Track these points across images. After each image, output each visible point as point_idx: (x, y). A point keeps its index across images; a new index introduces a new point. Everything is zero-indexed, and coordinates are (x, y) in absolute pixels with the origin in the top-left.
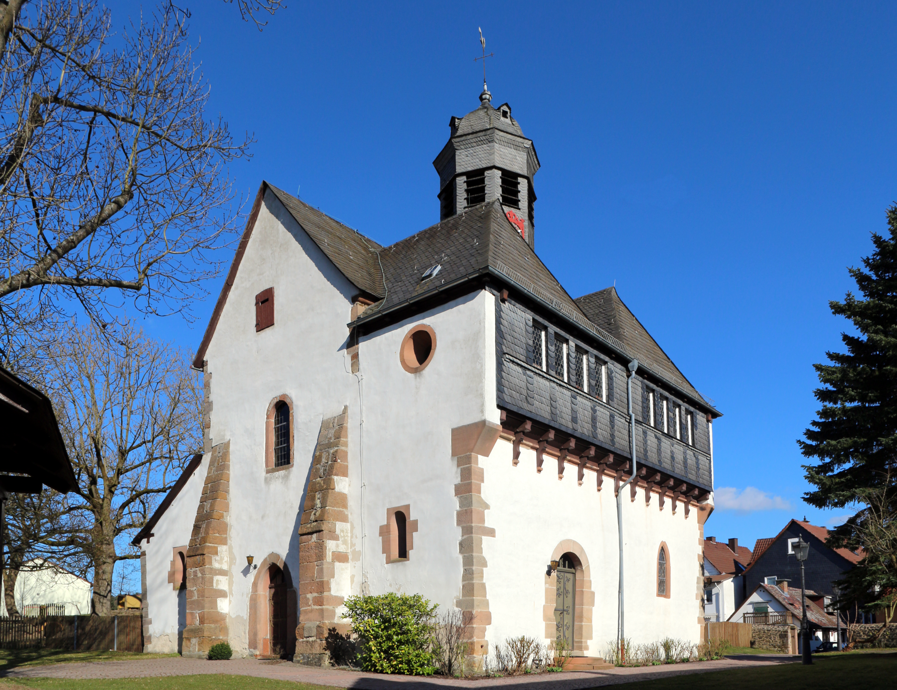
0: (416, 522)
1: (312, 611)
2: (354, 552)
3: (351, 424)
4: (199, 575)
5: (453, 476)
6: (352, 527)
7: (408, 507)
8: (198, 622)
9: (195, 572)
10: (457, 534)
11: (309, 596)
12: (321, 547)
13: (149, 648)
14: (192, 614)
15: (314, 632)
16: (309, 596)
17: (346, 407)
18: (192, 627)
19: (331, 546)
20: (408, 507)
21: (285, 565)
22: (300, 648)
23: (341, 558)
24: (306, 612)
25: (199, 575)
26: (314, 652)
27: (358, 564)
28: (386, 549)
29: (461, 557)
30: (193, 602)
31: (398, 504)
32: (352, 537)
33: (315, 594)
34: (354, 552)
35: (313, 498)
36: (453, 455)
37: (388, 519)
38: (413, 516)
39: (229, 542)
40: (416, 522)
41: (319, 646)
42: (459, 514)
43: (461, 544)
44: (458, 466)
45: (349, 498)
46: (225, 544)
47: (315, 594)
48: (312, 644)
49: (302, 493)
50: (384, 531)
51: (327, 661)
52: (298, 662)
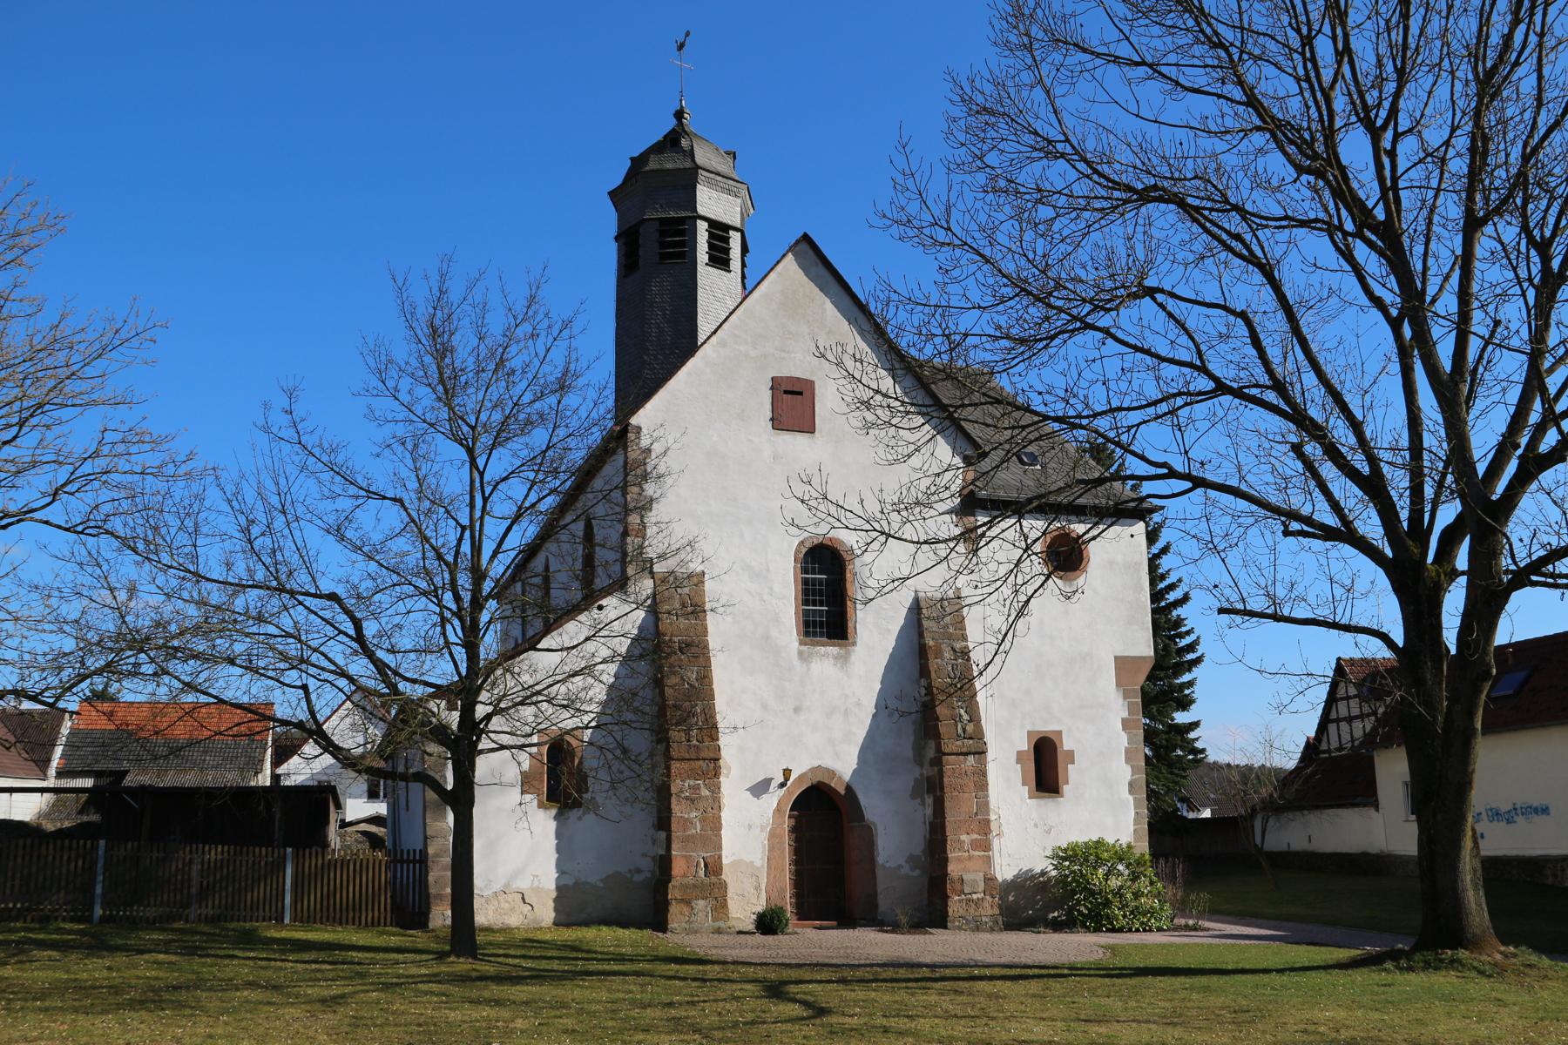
7: (1060, 733)
11: (964, 837)
14: (688, 858)
16: (964, 837)
18: (690, 880)
20: (1060, 733)
21: (849, 788)
22: (955, 906)
24: (959, 860)
25: (705, 792)
30: (687, 840)
33: (975, 836)
36: (1118, 685)
38: (1067, 744)
42: (1127, 751)
43: (1130, 784)
44: (1125, 698)
47: (975, 836)
48: (977, 903)
52: (960, 928)
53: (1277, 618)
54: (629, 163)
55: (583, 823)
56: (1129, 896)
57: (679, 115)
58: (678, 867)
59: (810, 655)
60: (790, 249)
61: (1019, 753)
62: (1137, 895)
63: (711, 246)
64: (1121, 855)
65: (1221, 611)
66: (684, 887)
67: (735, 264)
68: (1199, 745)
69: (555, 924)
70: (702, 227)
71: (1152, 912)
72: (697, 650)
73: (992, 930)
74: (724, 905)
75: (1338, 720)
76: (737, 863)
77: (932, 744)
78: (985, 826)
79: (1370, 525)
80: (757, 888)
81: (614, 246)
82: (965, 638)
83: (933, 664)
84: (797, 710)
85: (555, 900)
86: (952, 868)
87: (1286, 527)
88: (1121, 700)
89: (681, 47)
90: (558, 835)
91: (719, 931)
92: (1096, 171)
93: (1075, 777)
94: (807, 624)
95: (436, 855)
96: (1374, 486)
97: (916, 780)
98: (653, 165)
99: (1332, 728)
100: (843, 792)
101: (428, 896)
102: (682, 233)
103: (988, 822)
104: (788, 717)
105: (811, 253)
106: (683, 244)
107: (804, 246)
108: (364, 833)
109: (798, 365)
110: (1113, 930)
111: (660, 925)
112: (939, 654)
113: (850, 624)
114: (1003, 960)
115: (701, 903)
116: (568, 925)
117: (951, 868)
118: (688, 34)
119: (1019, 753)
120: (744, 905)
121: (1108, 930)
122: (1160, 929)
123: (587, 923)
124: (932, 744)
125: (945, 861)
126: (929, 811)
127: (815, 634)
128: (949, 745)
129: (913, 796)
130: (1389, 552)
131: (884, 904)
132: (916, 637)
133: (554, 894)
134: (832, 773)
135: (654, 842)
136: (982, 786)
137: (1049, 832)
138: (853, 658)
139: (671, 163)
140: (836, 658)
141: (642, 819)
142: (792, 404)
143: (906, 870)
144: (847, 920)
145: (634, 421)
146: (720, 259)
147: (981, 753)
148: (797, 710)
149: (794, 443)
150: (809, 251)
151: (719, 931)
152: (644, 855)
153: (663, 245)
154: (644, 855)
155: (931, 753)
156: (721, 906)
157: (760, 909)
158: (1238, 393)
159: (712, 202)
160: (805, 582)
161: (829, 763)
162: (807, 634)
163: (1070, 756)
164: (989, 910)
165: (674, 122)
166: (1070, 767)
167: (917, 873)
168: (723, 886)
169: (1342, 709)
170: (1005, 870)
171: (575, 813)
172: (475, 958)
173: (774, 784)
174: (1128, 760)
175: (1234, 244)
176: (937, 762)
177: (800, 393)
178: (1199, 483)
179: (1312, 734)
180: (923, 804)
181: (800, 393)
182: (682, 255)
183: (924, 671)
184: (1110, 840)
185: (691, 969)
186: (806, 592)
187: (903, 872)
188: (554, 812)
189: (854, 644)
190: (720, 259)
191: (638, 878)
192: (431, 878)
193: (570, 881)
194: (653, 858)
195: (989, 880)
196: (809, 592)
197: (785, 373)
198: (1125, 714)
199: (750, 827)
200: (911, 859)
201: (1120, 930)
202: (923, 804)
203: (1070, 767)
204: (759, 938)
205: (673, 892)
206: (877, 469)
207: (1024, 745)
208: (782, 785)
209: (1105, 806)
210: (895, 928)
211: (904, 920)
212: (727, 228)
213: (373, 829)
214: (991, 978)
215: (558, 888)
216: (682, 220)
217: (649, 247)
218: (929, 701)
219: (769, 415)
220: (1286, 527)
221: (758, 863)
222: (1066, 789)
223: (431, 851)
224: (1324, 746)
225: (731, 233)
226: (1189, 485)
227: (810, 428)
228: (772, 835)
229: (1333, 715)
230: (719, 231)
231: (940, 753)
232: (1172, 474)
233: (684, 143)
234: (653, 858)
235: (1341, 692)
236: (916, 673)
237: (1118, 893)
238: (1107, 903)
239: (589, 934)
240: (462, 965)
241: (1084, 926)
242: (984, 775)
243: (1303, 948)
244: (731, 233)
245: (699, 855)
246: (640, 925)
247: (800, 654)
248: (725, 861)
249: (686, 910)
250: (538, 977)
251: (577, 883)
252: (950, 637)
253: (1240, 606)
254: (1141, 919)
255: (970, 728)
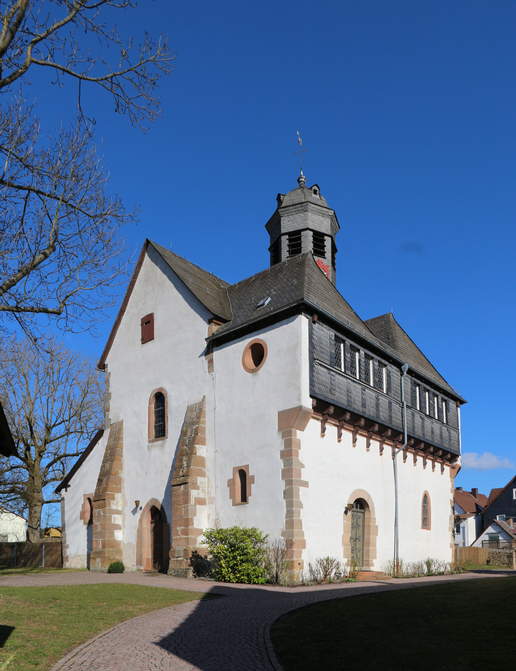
0: (253, 477)
1: (180, 539)
2: (210, 498)
3: (208, 408)
4: (102, 514)
5: (279, 445)
6: (209, 481)
7: (247, 466)
8: (101, 547)
9: (99, 512)
10: (282, 485)
11: (179, 528)
12: (187, 494)
13: (67, 565)
14: (97, 541)
15: (182, 554)
16: (179, 528)
17: (204, 397)
18: (97, 550)
19: (194, 494)
20: (247, 466)
21: (162, 507)
22: (172, 564)
23: (201, 502)
24: (176, 539)
26: (182, 568)
27: (213, 506)
28: (232, 496)
29: (284, 502)
31: (240, 464)
32: (208, 487)
33: (183, 528)
34: (210, 498)
35: (181, 460)
36: (279, 430)
37: (234, 475)
38: (251, 473)
39: (122, 491)
40: (253, 477)
41: (185, 564)
42: (283, 472)
43: (284, 492)
44: (283, 438)
45: (206, 460)
46: (120, 492)
47: (183, 528)
48: (181, 562)
49: (174, 456)
50: (231, 483)
51: (191, 574)
52: (171, 574)
100: (159, 509)
166: (252, 485)
203: (252, 485)
249: (94, 562)
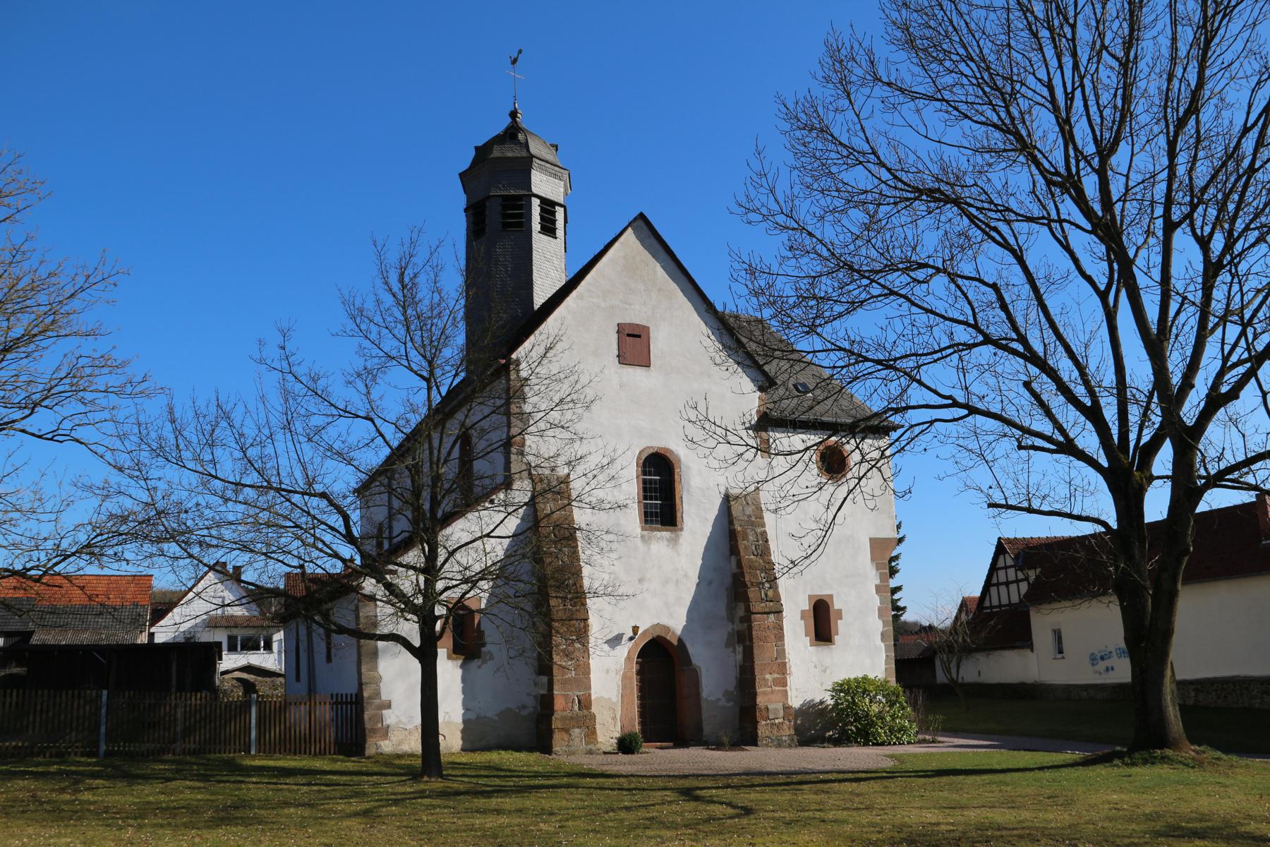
0: (840, 611)
7: (831, 596)
11: (768, 676)
14: (566, 697)
16: (768, 676)
18: (568, 713)
20: (831, 596)
21: (680, 640)
22: (763, 729)
24: (765, 693)
30: (565, 682)
33: (776, 675)
36: (873, 559)
38: (837, 605)
40: (840, 611)
42: (880, 609)
43: (882, 634)
47: (776, 675)
48: (779, 726)
49: (700, 562)
52: (767, 745)
53: (1030, 510)
54: (473, 153)
55: (483, 670)
56: (888, 719)
57: (513, 114)
58: (559, 704)
59: (650, 538)
60: (630, 225)
61: (803, 612)
62: (893, 717)
63: (542, 218)
64: (882, 687)
65: (990, 505)
66: (564, 719)
67: (560, 233)
68: (900, 604)
69: (463, 750)
70: (536, 203)
71: (902, 729)
72: (567, 535)
73: (790, 746)
74: (594, 732)
75: (998, 584)
76: (597, 699)
77: (742, 606)
78: (782, 668)
79: (1089, 440)
80: (614, 718)
81: (463, 215)
82: (763, 525)
83: (742, 545)
84: (641, 581)
85: (463, 731)
86: (761, 701)
87: (1020, 443)
88: (874, 571)
89: (514, 61)
90: (464, 680)
91: (590, 752)
92: (895, 177)
93: (844, 629)
94: (646, 514)
95: (370, 698)
96: (1093, 414)
97: (729, 634)
98: (496, 153)
99: (993, 590)
100: (675, 643)
101: (364, 730)
102: (521, 207)
103: (785, 664)
104: (640, 586)
105: (645, 228)
106: (521, 216)
107: (640, 223)
108: (238, 679)
109: (635, 316)
110: (877, 744)
111: (546, 748)
112: (745, 537)
113: (678, 515)
114: (865, 768)
115: (577, 730)
116: (473, 751)
117: (759, 700)
118: (520, 52)
119: (803, 612)
120: (608, 732)
121: (874, 744)
122: (909, 743)
123: (489, 749)
124: (742, 606)
125: (754, 695)
126: (740, 657)
127: (652, 522)
128: (757, 606)
129: (727, 646)
130: (1106, 464)
131: (707, 729)
132: (726, 524)
133: (461, 726)
134: (667, 629)
135: (536, 684)
136: (780, 637)
137: (825, 671)
138: (681, 541)
139: (511, 152)
140: (668, 540)
141: (524, 670)
142: (633, 344)
143: (723, 702)
144: (680, 740)
145: (514, 356)
146: (549, 228)
147: (779, 612)
148: (641, 581)
149: (635, 373)
150: (644, 226)
151: (590, 752)
152: (529, 695)
153: (505, 216)
154: (529, 695)
155: (741, 612)
156: (591, 733)
157: (618, 735)
158: (996, 343)
159: (543, 184)
160: (645, 482)
161: (665, 621)
162: (646, 522)
163: (839, 614)
164: (787, 732)
165: (509, 120)
167: (731, 704)
168: (593, 717)
169: (1002, 576)
170: (795, 702)
171: (476, 662)
172: (442, 776)
173: (625, 638)
174: (880, 616)
175: (994, 234)
176: (747, 618)
177: (639, 336)
178: (973, 411)
179: (977, 593)
180: (734, 652)
181: (639, 336)
182: (520, 225)
183: (734, 550)
184: (871, 676)
185: (608, 782)
186: (645, 490)
187: (720, 703)
188: (460, 662)
189: (682, 529)
190: (549, 228)
191: (524, 713)
192: (366, 716)
193: (472, 716)
194: (535, 697)
195: (787, 708)
196: (647, 490)
197: (628, 321)
198: (878, 582)
199: (608, 671)
200: (727, 694)
201: (882, 744)
202: (734, 652)
204: (622, 757)
205: (556, 723)
206: (693, 397)
207: (806, 605)
208: (631, 639)
209: (864, 655)
210: (719, 746)
211: (725, 740)
212: (553, 204)
213: (245, 676)
214: (840, 781)
215: (464, 722)
216: (520, 197)
217: (493, 217)
218: (738, 575)
219: (616, 352)
220: (1020, 443)
221: (614, 699)
222: (836, 638)
223: (365, 694)
224: (987, 604)
225: (557, 208)
226: (966, 412)
227: (647, 364)
228: (624, 677)
229: (994, 581)
230: (548, 206)
231: (748, 609)
232: (956, 404)
233: (521, 137)
234: (535, 697)
235: (1001, 563)
236: (728, 553)
237: (880, 716)
238: (873, 724)
239: (494, 757)
240: (436, 784)
241: (856, 742)
242: (782, 629)
243: (1023, 753)
244: (557, 208)
245: (575, 694)
246: (531, 750)
247: (642, 537)
248: (593, 697)
249: (565, 736)
250: (500, 791)
251: (478, 717)
252: (753, 524)
253: (1003, 502)
254: (896, 736)
255: (770, 593)
